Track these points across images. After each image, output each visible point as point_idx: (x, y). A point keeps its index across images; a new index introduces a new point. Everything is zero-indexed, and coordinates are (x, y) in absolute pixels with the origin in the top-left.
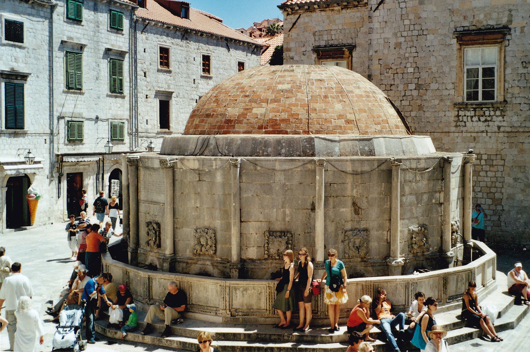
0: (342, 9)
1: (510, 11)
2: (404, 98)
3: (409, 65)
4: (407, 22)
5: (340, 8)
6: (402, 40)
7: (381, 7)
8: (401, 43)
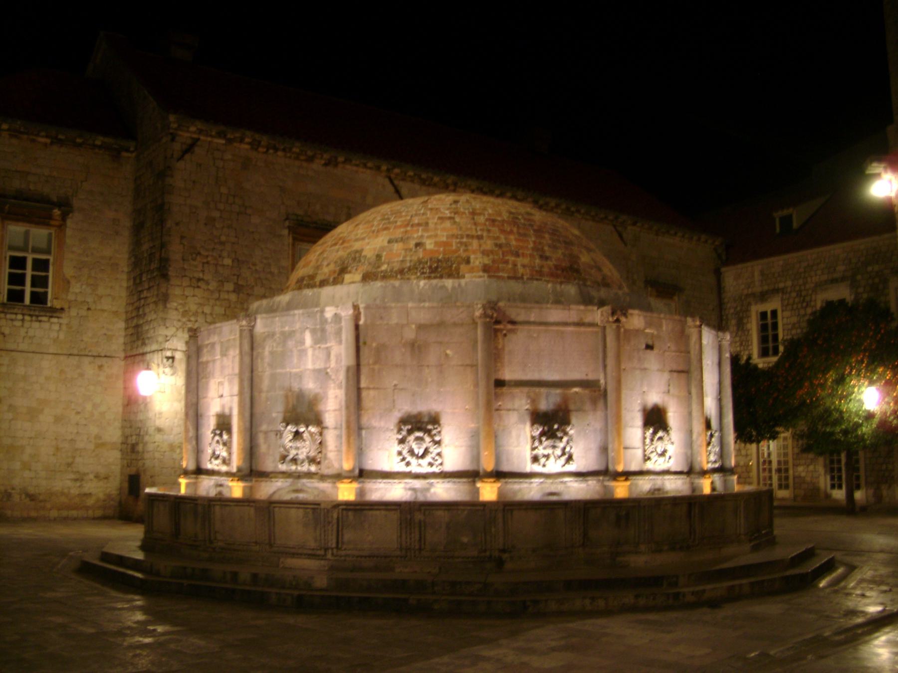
0: (52, 143)
1: (349, 208)
2: (218, 303)
3: (225, 254)
4: (224, 190)
5: (48, 141)
6: (216, 214)
7: (187, 157)
8: (214, 219)
